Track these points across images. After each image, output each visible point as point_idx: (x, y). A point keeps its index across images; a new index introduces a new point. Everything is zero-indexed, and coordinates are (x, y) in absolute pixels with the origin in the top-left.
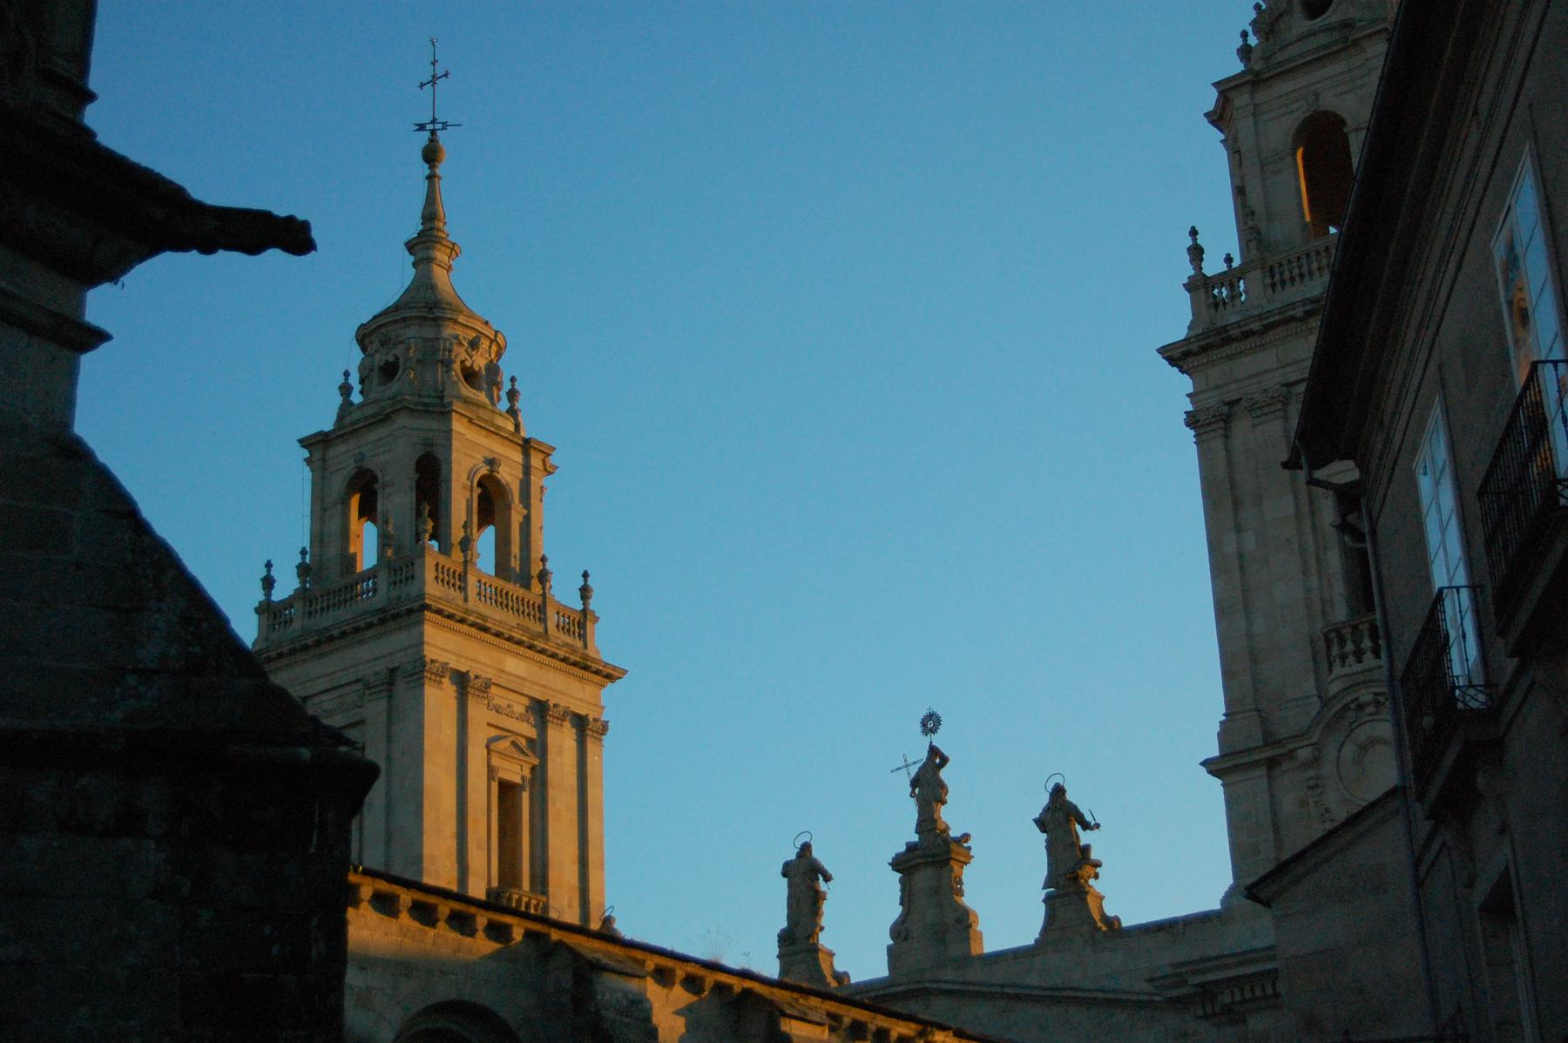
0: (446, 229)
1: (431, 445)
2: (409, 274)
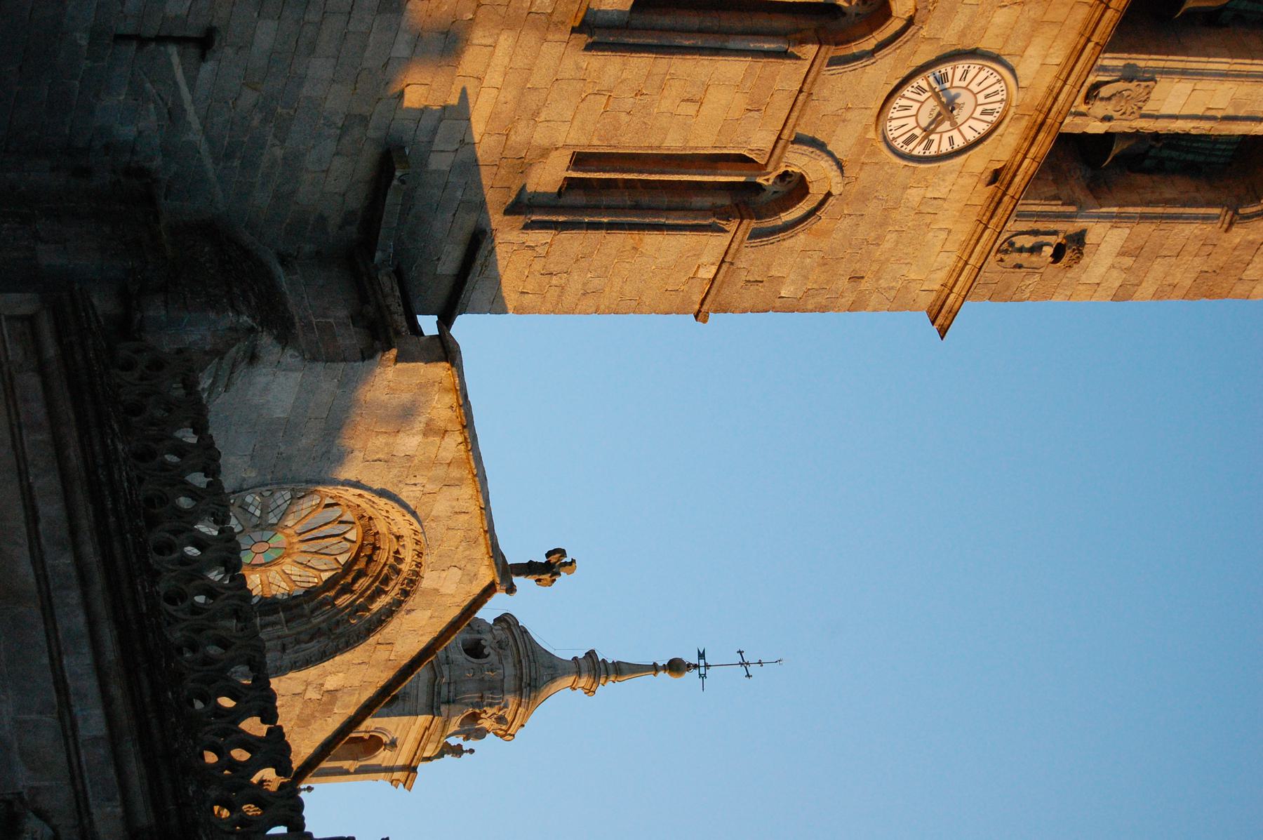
0: (609, 683)
1: (404, 700)
2: (567, 656)
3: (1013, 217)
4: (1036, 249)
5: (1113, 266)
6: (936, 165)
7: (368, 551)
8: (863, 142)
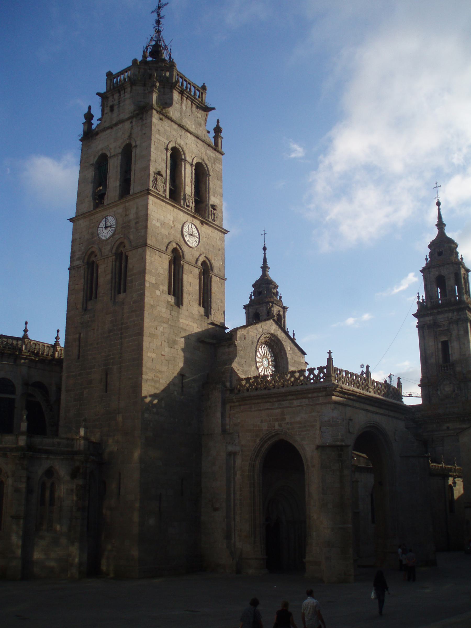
2: (261, 273)
3: (208, 219)
4: (214, 214)
5: (217, 198)
6: (200, 236)
7: (266, 343)
8: (197, 251)
